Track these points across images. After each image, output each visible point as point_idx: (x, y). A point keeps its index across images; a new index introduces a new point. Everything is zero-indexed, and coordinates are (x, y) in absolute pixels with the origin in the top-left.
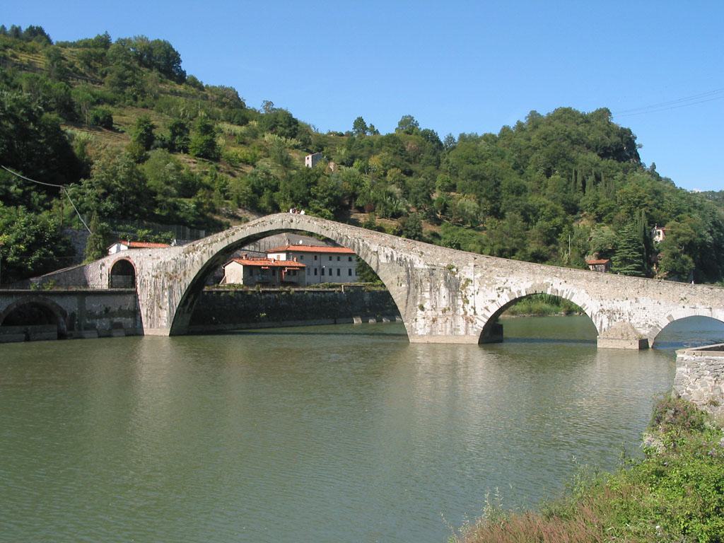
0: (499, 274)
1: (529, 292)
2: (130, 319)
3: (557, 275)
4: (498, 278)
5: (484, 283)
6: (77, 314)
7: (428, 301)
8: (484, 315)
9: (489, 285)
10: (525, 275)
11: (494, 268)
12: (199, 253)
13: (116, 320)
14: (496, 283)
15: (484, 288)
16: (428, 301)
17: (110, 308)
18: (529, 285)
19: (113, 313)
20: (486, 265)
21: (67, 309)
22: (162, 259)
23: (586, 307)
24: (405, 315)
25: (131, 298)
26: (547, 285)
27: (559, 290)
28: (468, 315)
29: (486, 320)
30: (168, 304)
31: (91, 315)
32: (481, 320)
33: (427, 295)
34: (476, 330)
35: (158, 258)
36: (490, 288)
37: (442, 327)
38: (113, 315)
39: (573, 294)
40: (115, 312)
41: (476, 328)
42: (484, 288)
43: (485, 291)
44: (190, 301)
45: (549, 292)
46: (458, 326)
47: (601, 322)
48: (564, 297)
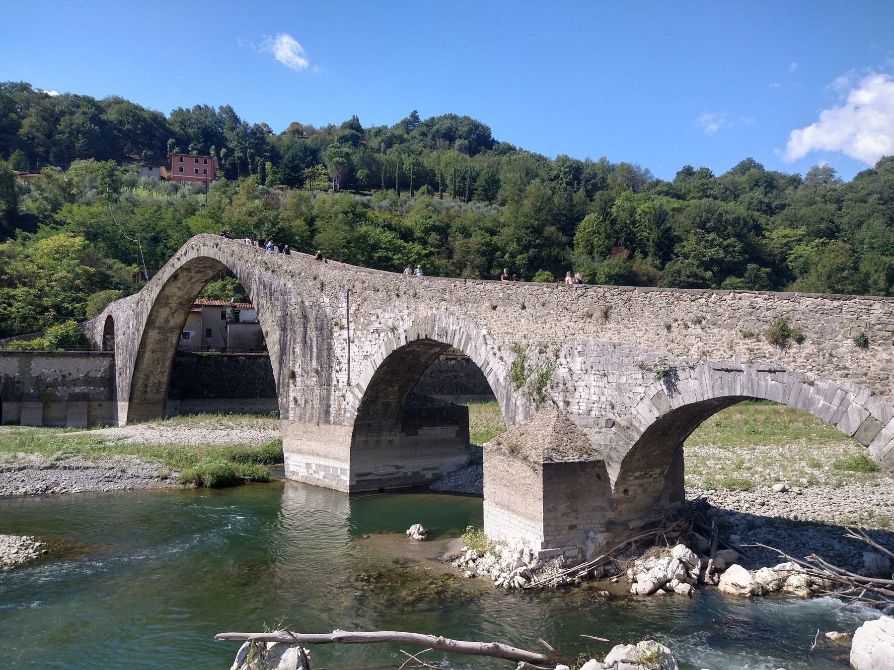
1: (412, 338)
2: (102, 389)
8: (358, 385)
13: (77, 390)
15: (359, 333)
17: (70, 374)
19: (74, 380)
23: (488, 370)
24: (279, 384)
25: (106, 362)
27: (449, 332)
29: (361, 396)
31: (39, 381)
32: (355, 396)
36: (365, 332)
40: (78, 379)
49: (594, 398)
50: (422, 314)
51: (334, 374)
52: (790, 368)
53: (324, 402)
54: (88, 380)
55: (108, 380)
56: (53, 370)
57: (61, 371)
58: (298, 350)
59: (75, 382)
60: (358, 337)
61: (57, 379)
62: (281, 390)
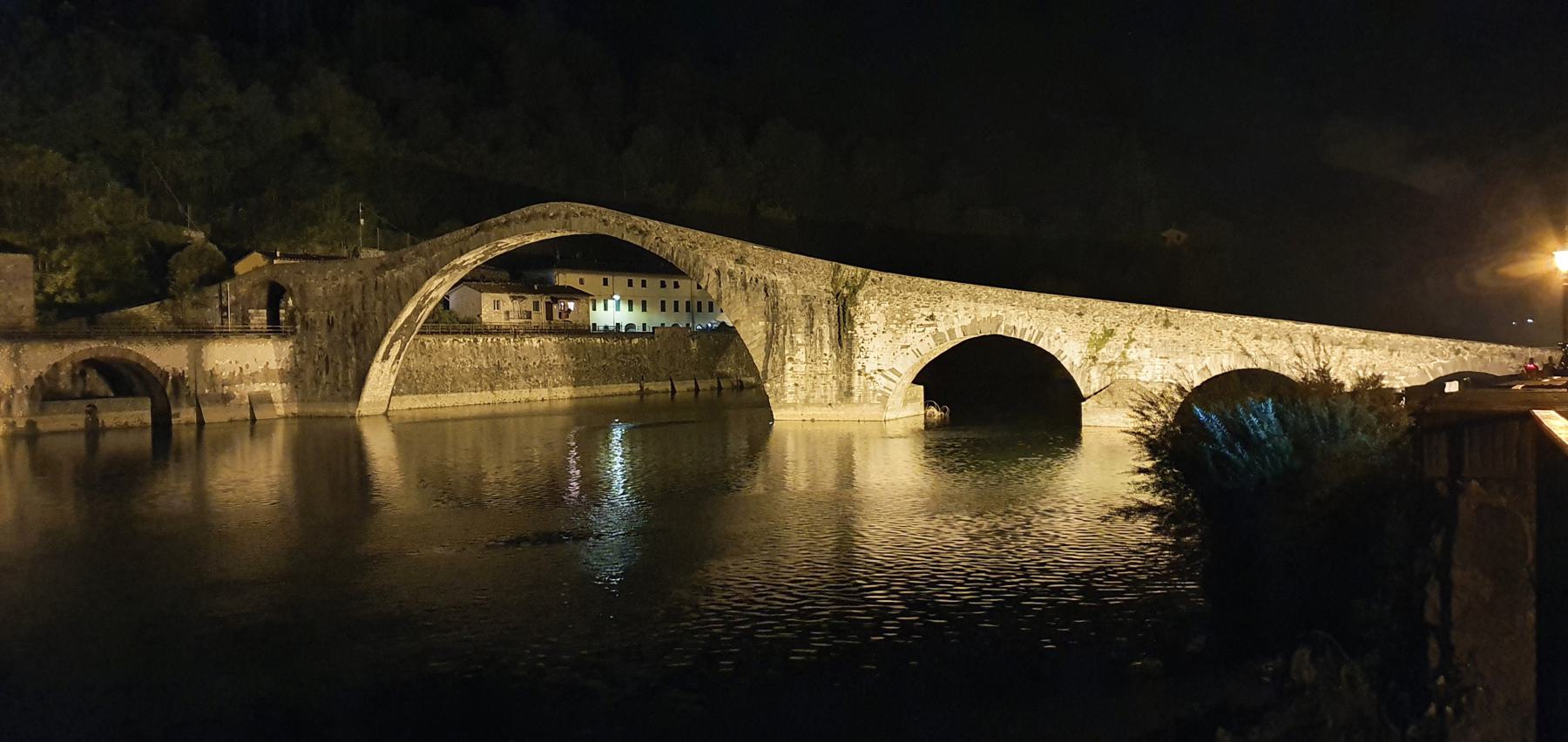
0: (918, 303)
3: (1016, 303)
4: (916, 310)
5: (893, 318)
6: (186, 376)
7: (803, 349)
9: (902, 322)
10: (961, 305)
11: (909, 293)
12: (408, 268)
14: (914, 319)
15: (894, 327)
16: (803, 349)
18: (968, 322)
20: (896, 288)
21: (167, 369)
22: (342, 281)
23: (1062, 356)
24: (765, 371)
26: (999, 318)
27: (1019, 329)
28: (867, 371)
30: (354, 359)
33: (799, 339)
34: (880, 395)
35: (335, 278)
36: (904, 326)
37: (825, 391)
38: (253, 377)
39: (1041, 335)
40: (257, 372)
41: (881, 392)
42: (894, 327)
43: (895, 332)
44: (394, 352)
45: (1001, 332)
46: (852, 388)
47: (1088, 380)
48: (1025, 339)
49: (1158, 372)
50: (985, 314)
51: (856, 361)
52: (1276, 354)
53: (846, 384)
54: (267, 375)
55: (288, 373)
56: (228, 361)
57: (236, 362)
58: (799, 339)
59: (253, 377)
60: (891, 329)
61: (234, 373)
62: (770, 375)
